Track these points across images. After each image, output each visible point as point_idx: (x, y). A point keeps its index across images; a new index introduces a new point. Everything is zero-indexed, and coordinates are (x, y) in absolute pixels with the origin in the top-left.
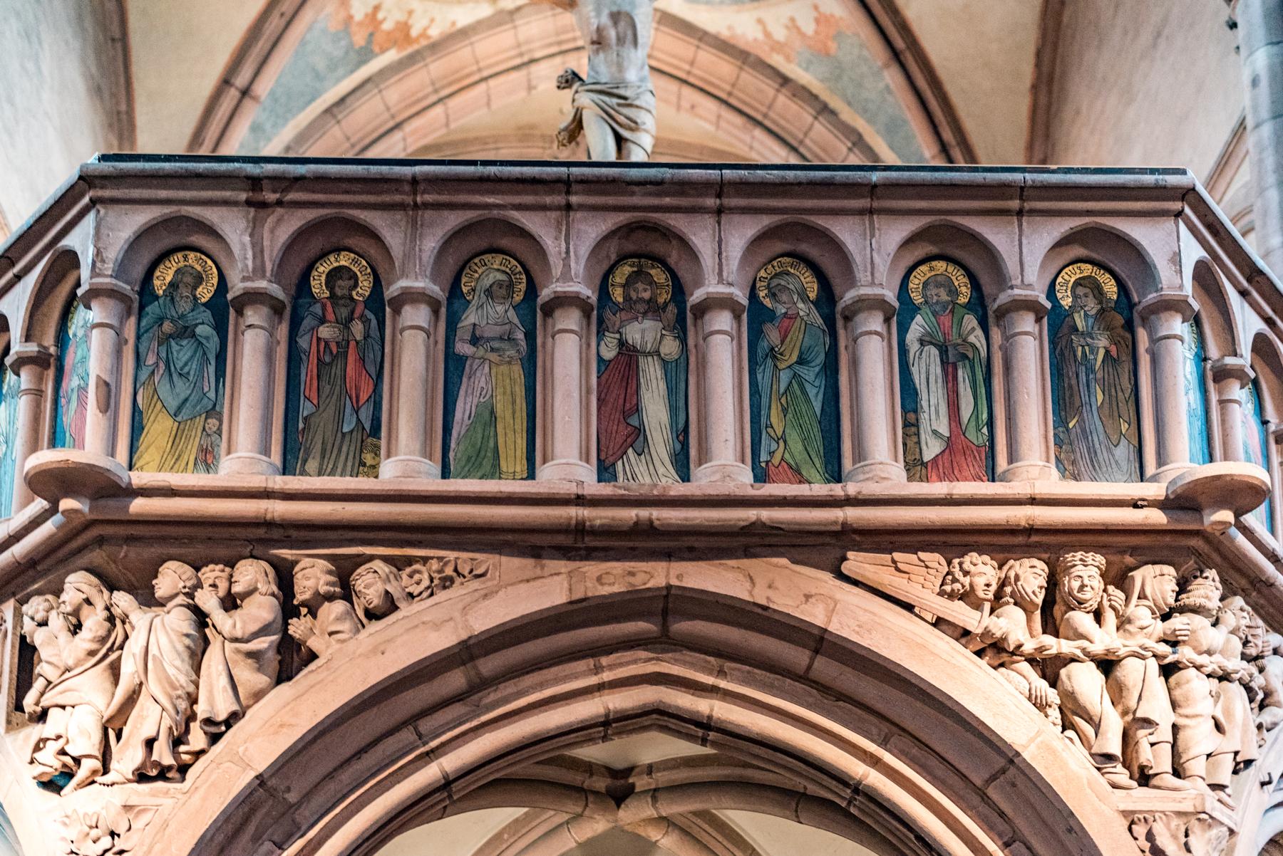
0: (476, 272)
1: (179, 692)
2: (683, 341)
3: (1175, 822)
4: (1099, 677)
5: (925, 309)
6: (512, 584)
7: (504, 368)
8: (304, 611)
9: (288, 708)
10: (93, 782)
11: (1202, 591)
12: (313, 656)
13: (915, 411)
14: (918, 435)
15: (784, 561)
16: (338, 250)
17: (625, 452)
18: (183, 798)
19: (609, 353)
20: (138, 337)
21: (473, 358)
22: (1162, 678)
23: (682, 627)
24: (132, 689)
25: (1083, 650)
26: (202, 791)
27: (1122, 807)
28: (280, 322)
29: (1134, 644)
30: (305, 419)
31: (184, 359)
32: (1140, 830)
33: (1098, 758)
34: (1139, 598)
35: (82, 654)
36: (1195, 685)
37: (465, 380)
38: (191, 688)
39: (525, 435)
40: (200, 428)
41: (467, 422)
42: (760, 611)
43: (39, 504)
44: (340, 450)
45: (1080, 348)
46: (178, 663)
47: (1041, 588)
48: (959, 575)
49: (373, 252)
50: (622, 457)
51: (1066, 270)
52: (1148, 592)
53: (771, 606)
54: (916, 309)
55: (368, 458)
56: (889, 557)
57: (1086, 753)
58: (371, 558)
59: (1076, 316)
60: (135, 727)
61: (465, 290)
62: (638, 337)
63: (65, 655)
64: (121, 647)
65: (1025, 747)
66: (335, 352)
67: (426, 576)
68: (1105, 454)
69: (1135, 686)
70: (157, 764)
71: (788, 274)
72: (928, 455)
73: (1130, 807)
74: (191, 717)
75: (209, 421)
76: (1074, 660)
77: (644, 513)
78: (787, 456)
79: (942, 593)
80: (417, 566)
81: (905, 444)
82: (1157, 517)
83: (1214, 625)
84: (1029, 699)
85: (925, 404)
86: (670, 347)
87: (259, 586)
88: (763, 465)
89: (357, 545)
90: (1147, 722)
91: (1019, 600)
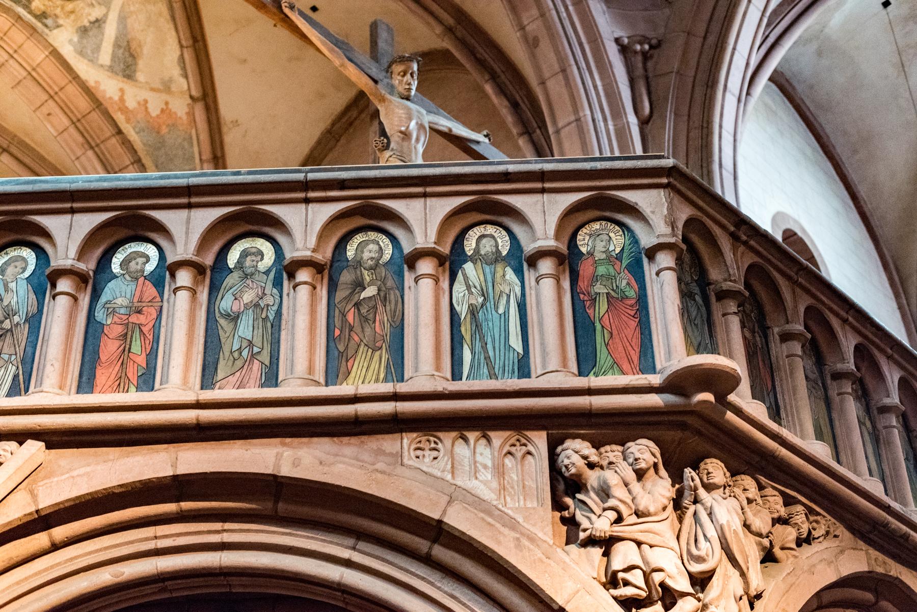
87: (756, 498)
89: (794, 491)
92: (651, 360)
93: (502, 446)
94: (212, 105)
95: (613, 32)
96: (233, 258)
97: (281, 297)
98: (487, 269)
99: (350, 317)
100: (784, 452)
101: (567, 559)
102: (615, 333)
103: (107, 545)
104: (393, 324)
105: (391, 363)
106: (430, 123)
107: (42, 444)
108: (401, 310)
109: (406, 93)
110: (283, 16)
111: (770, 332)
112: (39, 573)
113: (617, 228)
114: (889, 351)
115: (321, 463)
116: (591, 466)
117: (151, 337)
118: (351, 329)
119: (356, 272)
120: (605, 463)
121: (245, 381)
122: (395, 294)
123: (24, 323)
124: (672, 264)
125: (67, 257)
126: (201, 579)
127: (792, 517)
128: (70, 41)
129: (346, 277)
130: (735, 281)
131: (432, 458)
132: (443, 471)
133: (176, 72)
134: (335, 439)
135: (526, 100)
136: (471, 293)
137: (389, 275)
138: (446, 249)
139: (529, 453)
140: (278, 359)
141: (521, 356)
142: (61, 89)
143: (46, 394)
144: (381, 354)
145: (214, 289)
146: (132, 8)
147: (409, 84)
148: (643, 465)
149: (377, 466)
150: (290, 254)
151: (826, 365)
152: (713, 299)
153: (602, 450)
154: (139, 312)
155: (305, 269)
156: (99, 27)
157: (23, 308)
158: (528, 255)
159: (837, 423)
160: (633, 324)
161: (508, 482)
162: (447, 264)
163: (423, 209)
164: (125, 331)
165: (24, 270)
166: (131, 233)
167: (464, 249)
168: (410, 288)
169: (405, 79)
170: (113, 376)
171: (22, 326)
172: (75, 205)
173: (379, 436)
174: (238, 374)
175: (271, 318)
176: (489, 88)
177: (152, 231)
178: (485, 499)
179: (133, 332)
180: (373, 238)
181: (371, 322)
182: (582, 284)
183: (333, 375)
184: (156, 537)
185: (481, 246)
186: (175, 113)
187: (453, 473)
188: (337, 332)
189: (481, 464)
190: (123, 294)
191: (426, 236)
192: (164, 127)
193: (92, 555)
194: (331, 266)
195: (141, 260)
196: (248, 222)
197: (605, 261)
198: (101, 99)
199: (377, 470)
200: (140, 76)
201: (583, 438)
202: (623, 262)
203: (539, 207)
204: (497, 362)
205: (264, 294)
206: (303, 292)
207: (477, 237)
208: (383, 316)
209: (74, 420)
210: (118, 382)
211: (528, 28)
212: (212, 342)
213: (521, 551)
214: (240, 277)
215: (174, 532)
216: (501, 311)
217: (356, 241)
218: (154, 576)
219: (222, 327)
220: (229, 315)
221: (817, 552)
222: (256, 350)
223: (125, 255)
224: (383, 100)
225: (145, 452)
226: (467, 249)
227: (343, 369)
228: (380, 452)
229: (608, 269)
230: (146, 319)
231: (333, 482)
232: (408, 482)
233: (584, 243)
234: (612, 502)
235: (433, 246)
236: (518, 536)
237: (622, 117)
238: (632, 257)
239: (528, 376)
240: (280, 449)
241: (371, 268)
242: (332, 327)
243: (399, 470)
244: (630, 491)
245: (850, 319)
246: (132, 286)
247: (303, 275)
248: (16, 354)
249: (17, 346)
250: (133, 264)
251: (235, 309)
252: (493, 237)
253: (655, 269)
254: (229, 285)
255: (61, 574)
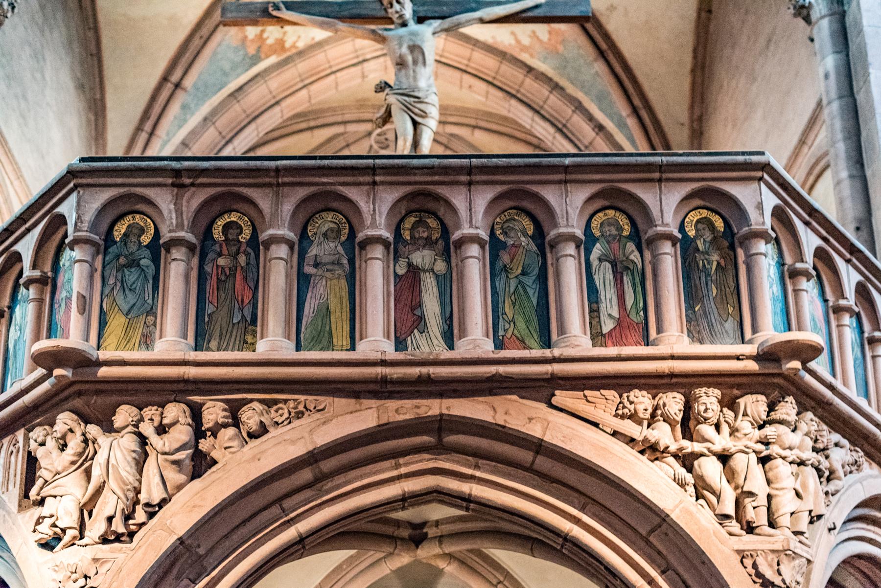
0: (317, 223)
1: (129, 487)
2: (448, 261)
3: (771, 556)
4: (719, 466)
5: (602, 239)
6: (342, 415)
7: (335, 281)
8: (209, 433)
9: (198, 495)
10: (74, 544)
11: (784, 411)
12: (214, 462)
13: (597, 303)
14: (599, 317)
15: (515, 397)
16: (230, 211)
17: (412, 332)
18: (132, 553)
19: (401, 270)
20: (104, 267)
21: (315, 275)
22: (760, 465)
23: (451, 439)
24: (99, 485)
25: (708, 449)
26: (143, 549)
27: (736, 548)
28: (194, 255)
29: (740, 445)
30: (209, 315)
31: (133, 280)
32: (748, 562)
33: (719, 517)
34: (743, 415)
35: (67, 464)
36: (782, 469)
37: (310, 289)
38: (137, 484)
39: (348, 322)
40: (143, 322)
41: (312, 315)
42: (500, 429)
43: (40, 372)
44: (231, 333)
45: (701, 262)
46: (128, 469)
47: (680, 411)
48: (627, 404)
49: (252, 212)
50: (410, 335)
51: (691, 213)
52: (749, 412)
53: (507, 425)
54: (595, 240)
55: (249, 339)
56: (582, 393)
57: (712, 513)
58: (252, 401)
59: (698, 242)
60: (100, 509)
61: (310, 234)
62: (419, 261)
63: (56, 464)
64: (92, 459)
65: (672, 511)
66: (228, 274)
67: (286, 411)
68: (719, 327)
69: (742, 471)
70: (115, 532)
71: (515, 220)
72: (606, 330)
73: (742, 548)
74: (137, 502)
75: (148, 317)
76: (702, 455)
77: (424, 370)
78: (516, 332)
79: (616, 415)
80: (280, 405)
81: (591, 323)
82: (752, 366)
83: (793, 431)
84: (674, 480)
85: (603, 298)
86: (440, 266)
87: (180, 419)
88: (501, 338)
89: (243, 393)
90: (751, 494)
91: (666, 419)
142: (469, 60)
198: (504, 50)
245: (378, 179)
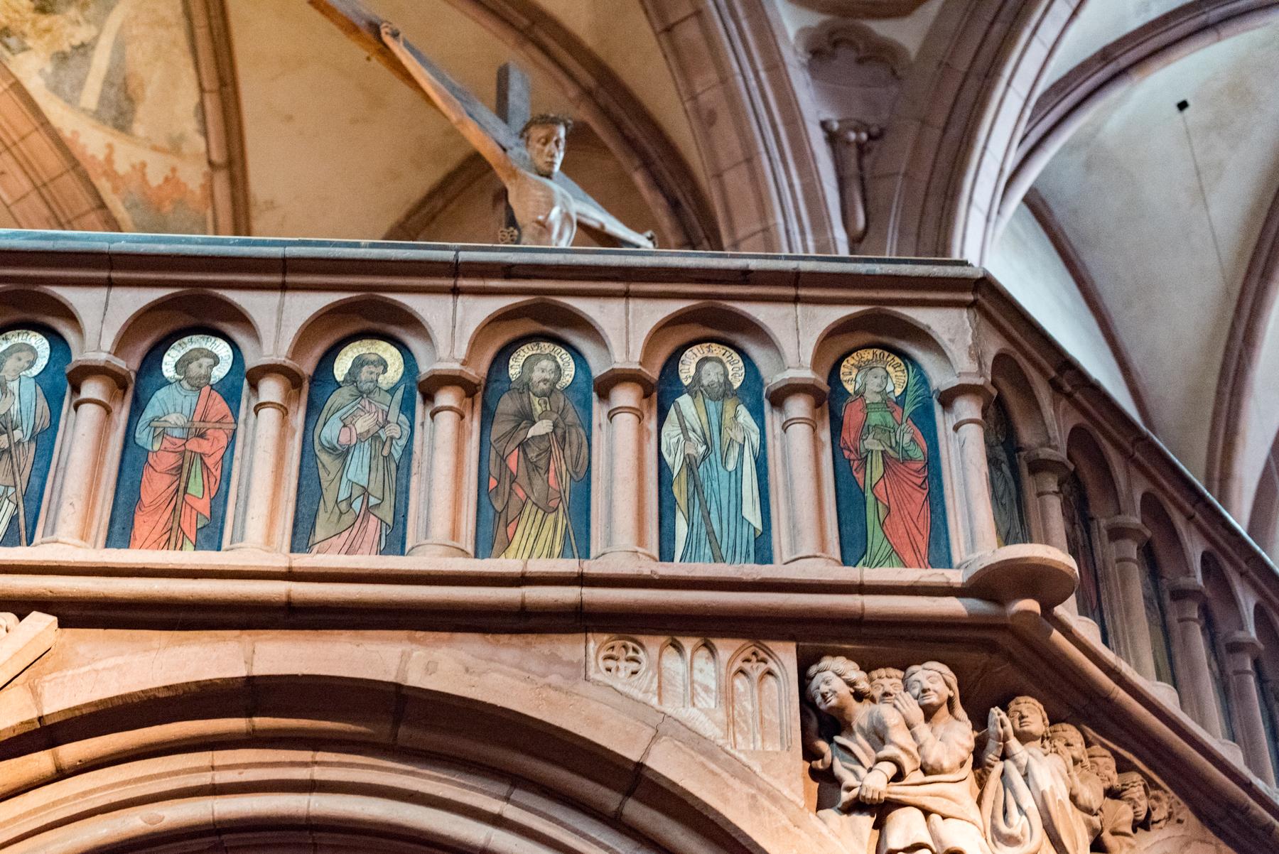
87: (1083, 758)
92: (945, 550)
93: (731, 661)
94: (239, 178)
95: (818, 112)
96: (342, 367)
97: (412, 427)
98: (712, 406)
99: (512, 462)
100: (1122, 695)
101: (824, 830)
102: (894, 507)
103: (139, 775)
104: (573, 475)
105: (571, 533)
106: (578, 214)
107: (52, 620)
108: (587, 456)
109: (546, 168)
110: (381, 46)
111: (1094, 525)
112: (37, 811)
113: (897, 360)
114: (1244, 566)
115: (467, 670)
116: (859, 696)
117: (218, 473)
118: (513, 479)
119: (521, 398)
120: (877, 694)
121: (356, 544)
122: (578, 434)
123: (29, 441)
124: (978, 415)
125: (99, 349)
126: (276, 834)
127: (1125, 790)
128: (41, 72)
129: (507, 405)
130: (1056, 448)
131: (629, 672)
132: (646, 692)
133: (190, 126)
134: (489, 636)
135: (690, 199)
136: (687, 439)
137: (569, 406)
138: (653, 373)
139: (770, 673)
140: (405, 517)
141: (759, 533)
142: (23, 138)
143: (61, 546)
144: (557, 517)
145: (313, 410)
146: (135, 32)
147: (553, 156)
148: (934, 699)
149: (547, 680)
150: (426, 367)
151: (1164, 578)
152: (1025, 470)
153: (875, 674)
154: (201, 435)
155: (450, 388)
156: (85, 55)
157: (28, 419)
158: (773, 389)
159: (1178, 660)
160: (920, 496)
161: (739, 712)
162: (655, 394)
163: (623, 314)
164: (181, 462)
165: (31, 364)
166: (191, 321)
167: (678, 375)
168: (600, 425)
169: (547, 149)
170: (160, 526)
171: (26, 446)
172: (114, 275)
173: (555, 636)
174: (345, 534)
175: (397, 456)
176: (639, 179)
177: (222, 320)
178: (707, 736)
179: (191, 465)
180: (547, 352)
181: (542, 472)
182: (848, 436)
183: (484, 544)
184: (213, 768)
185: (703, 372)
186: (185, 185)
187: (660, 695)
188: (493, 483)
189: (701, 685)
190: (179, 409)
191: (628, 352)
192: (167, 203)
193: (116, 790)
194: (486, 388)
195: (206, 362)
196: (367, 318)
197: (880, 406)
198: (79, 158)
199: (550, 686)
200: (139, 129)
201: (849, 655)
202: (906, 408)
203: (790, 322)
204: (725, 539)
205: (387, 422)
206: (446, 421)
207: (697, 360)
208: (560, 466)
209: (104, 586)
210: (166, 537)
211: (703, 98)
212: (309, 486)
213: (758, 814)
214: (352, 395)
215: (239, 761)
216: (731, 467)
217: (522, 353)
218: (207, 824)
219: (324, 466)
220: (334, 449)
221: (1158, 841)
222: (373, 501)
223: (183, 352)
224: (513, 174)
225: (206, 639)
226: (682, 376)
227: (500, 536)
228: (554, 659)
229: (884, 418)
230: (212, 447)
231: (484, 699)
232: (594, 705)
233: (851, 378)
234: (889, 751)
235: (638, 367)
236: (753, 791)
237: (826, 231)
238: (917, 403)
239: (769, 560)
240: (406, 647)
241: (543, 394)
242: (485, 474)
243: (582, 687)
244: (914, 736)
245: (1198, 516)
246: (192, 397)
247: (446, 398)
248: (15, 486)
249: (17, 475)
250: (194, 367)
251: (344, 439)
252: (721, 361)
253: (952, 421)
254: (335, 405)
255: (68, 814)
